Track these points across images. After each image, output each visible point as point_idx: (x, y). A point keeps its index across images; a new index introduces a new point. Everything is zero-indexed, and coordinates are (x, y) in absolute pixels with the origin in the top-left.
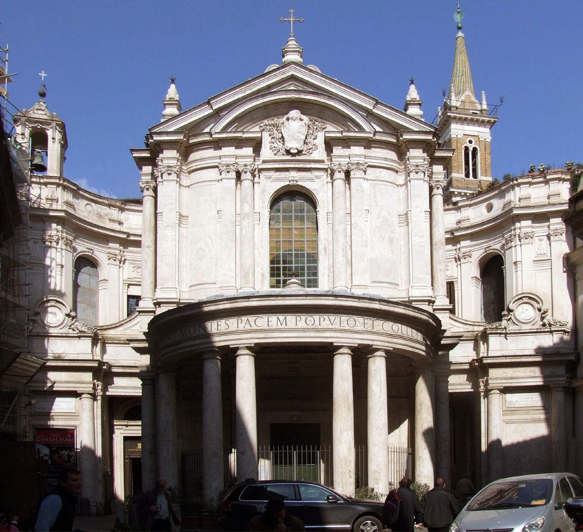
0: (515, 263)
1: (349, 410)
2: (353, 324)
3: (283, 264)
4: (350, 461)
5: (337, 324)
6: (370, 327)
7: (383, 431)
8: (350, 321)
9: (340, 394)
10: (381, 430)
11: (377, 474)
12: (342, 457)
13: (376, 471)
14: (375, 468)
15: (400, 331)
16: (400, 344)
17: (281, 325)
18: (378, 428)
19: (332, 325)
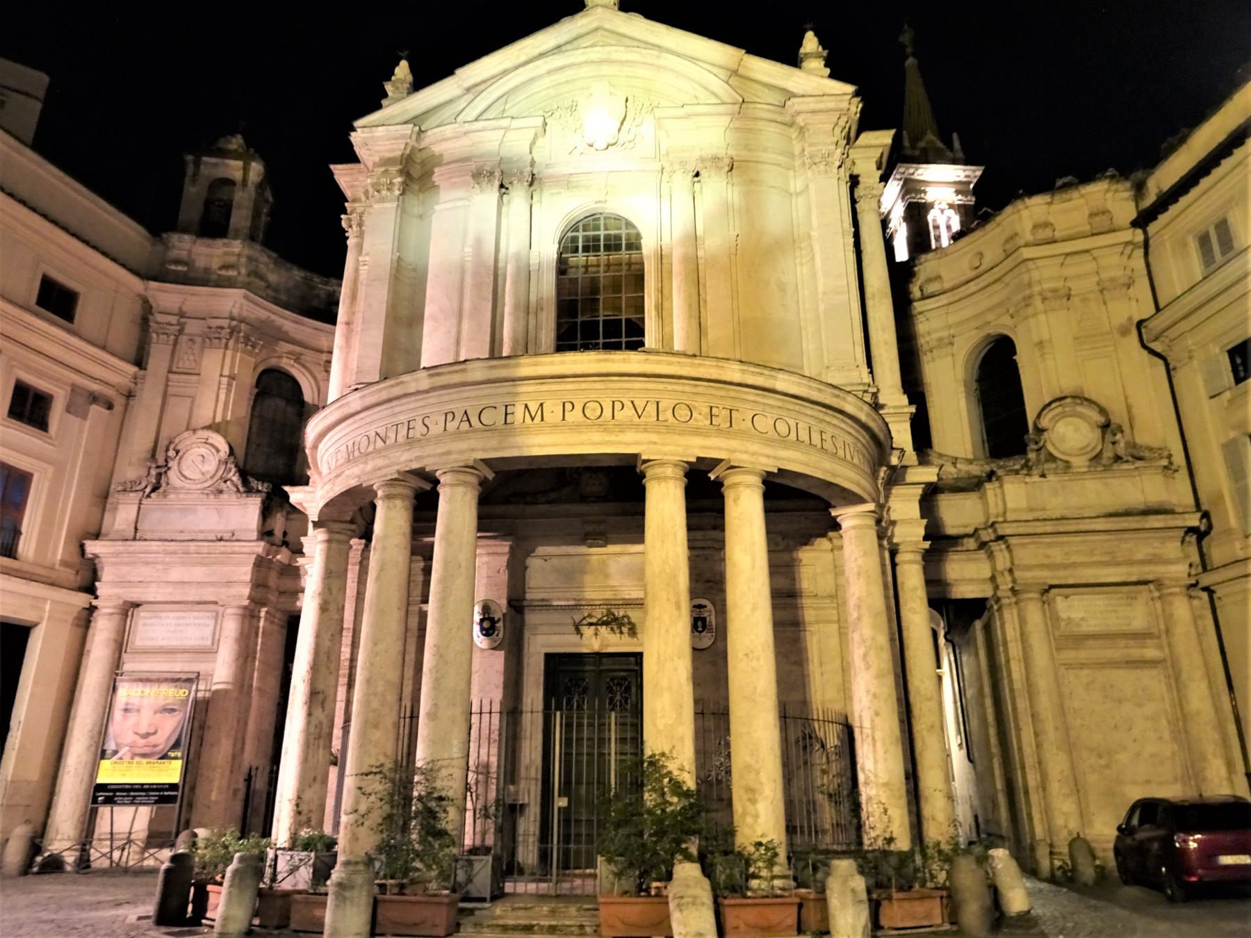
0: (1040, 344)
1: (678, 608)
2: (686, 415)
3: (576, 339)
4: (682, 739)
5: (650, 416)
6: (726, 422)
7: (762, 662)
8: (680, 409)
9: (657, 570)
10: (758, 659)
11: (752, 776)
12: (662, 728)
13: (748, 767)
14: (748, 759)
15: (793, 434)
16: (796, 461)
17: (533, 419)
18: (751, 656)
19: (639, 417)
